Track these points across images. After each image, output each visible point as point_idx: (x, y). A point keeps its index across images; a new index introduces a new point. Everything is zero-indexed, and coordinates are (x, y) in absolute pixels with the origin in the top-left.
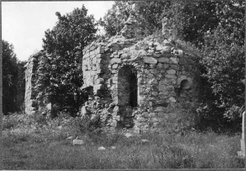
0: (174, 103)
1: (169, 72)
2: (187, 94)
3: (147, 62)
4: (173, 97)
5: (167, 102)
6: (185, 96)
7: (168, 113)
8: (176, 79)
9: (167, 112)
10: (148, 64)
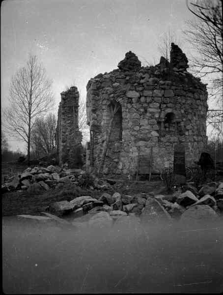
0: (156, 137)
1: (151, 105)
3: (129, 96)
4: (156, 131)
8: (160, 112)
10: (131, 98)
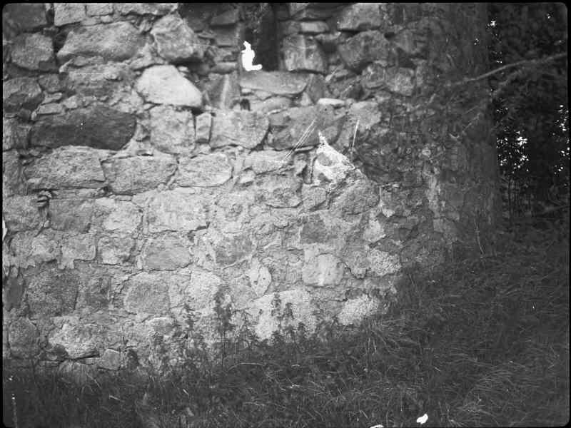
0: (185, 108)
2: (327, 50)
4: (177, 63)
5: (125, 108)
6: (308, 64)
7: (130, 193)
9: (117, 187)
